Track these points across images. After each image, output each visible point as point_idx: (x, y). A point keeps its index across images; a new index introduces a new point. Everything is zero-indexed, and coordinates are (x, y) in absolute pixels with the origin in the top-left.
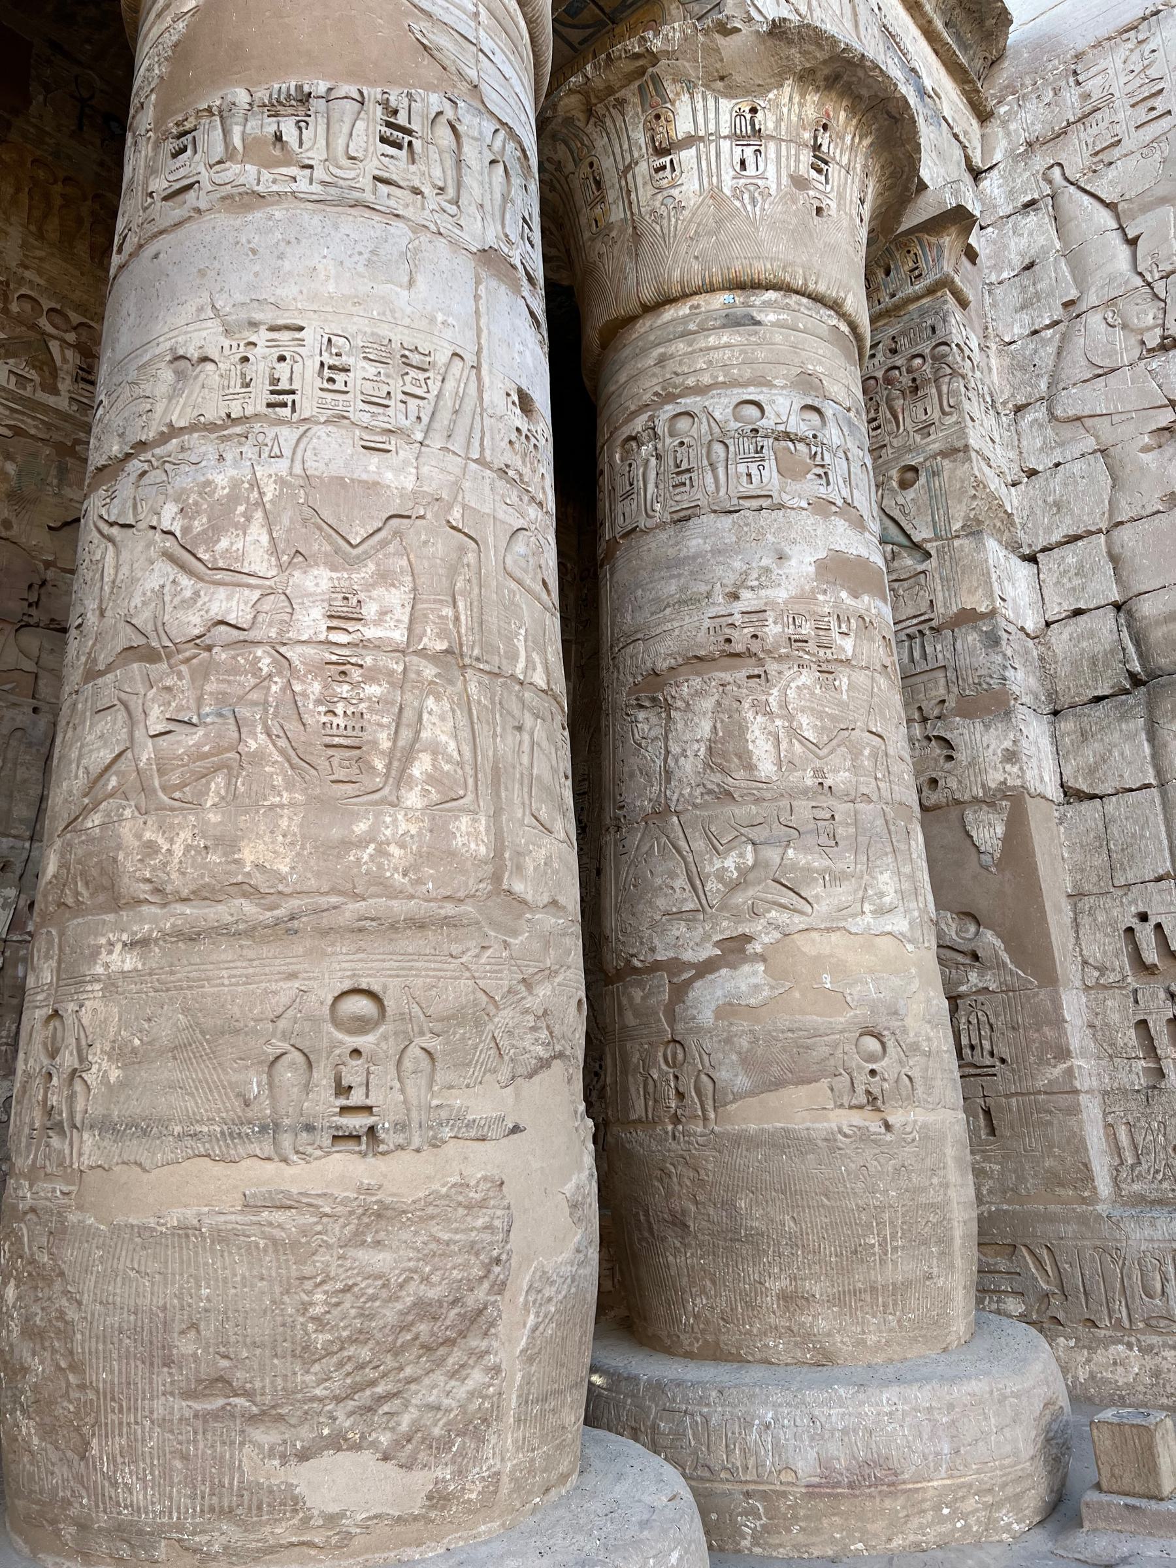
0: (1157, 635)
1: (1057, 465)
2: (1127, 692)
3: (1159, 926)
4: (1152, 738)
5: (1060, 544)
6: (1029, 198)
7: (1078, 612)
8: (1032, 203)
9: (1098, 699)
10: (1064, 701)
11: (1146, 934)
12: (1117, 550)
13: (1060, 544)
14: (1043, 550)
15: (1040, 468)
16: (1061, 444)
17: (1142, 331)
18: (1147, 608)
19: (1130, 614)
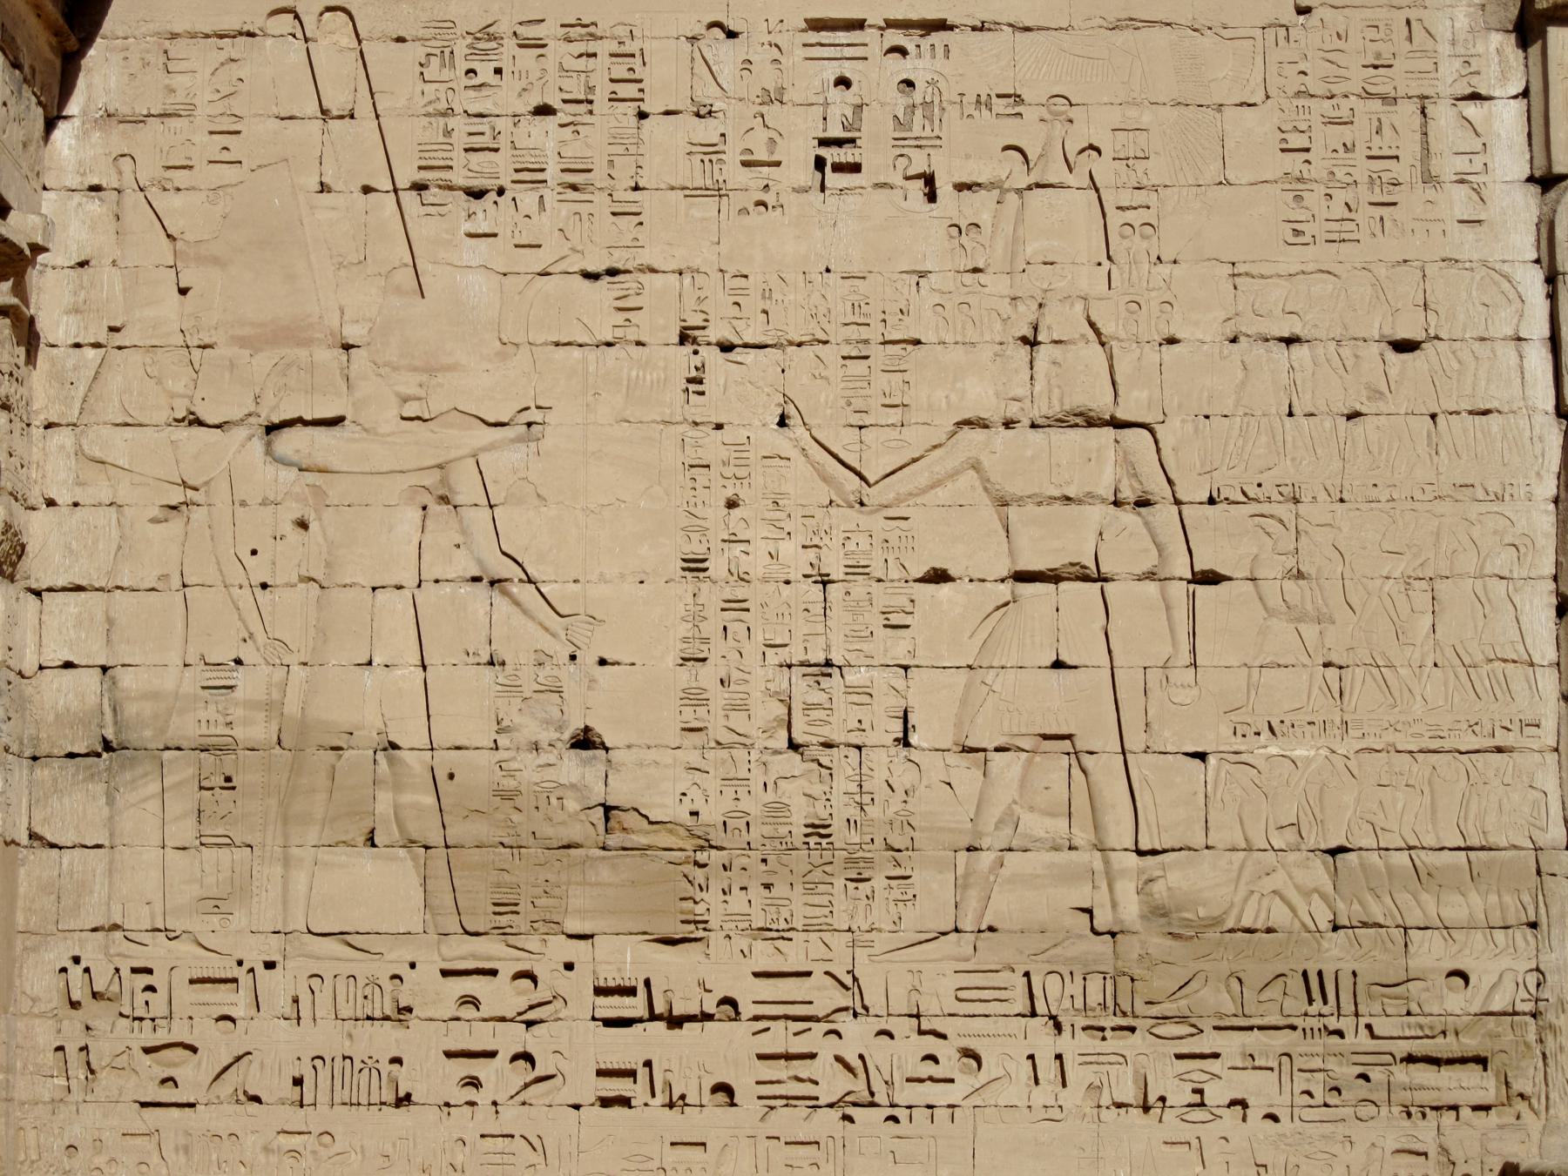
0: (131, 710)
1: (76, 505)
2: (99, 755)
3: (87, 970)
4: (111, 801)
5: (64, 589)
6: (95, 181)
7: (68, 665)
8: (96, 188)
9: (71, 755)
10: (44, 749)
11: (76, 972)
12: (112, 614)
13: (64, 589)
14: (50, 590)
15: (59, 501)
16: (79, 483)
17: (172, 396)
18: (127, 679)
19: (114, 682)
